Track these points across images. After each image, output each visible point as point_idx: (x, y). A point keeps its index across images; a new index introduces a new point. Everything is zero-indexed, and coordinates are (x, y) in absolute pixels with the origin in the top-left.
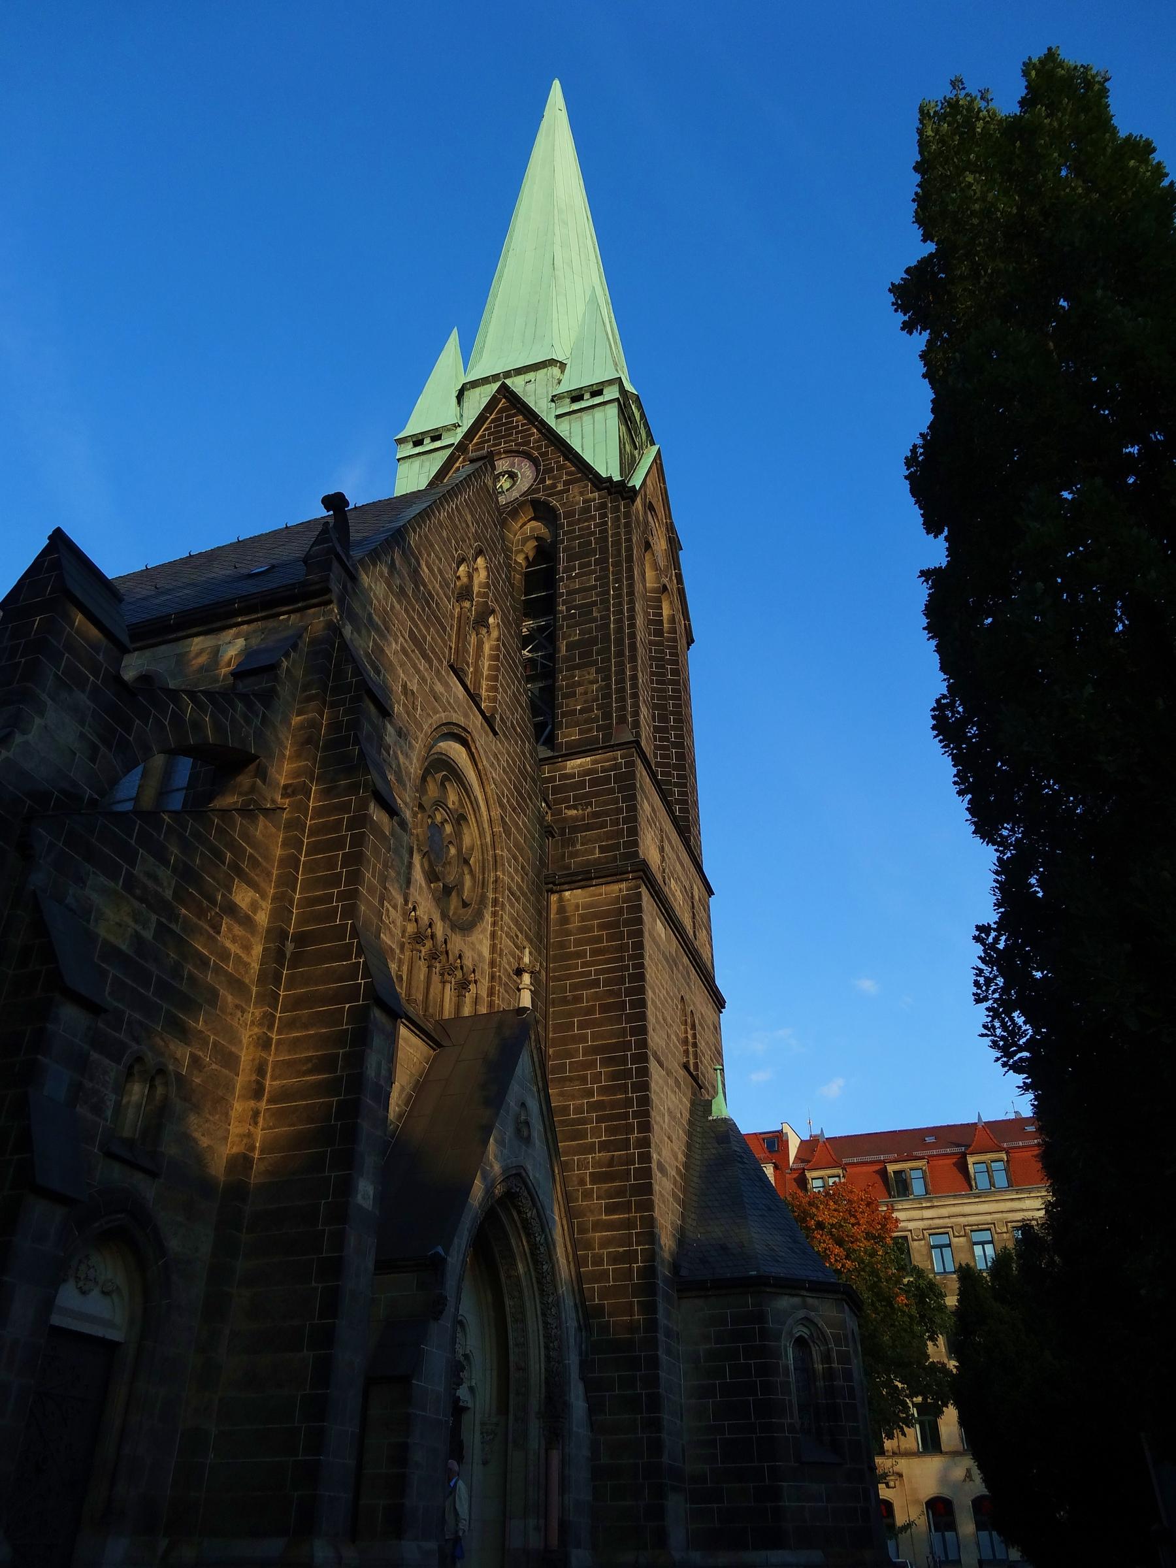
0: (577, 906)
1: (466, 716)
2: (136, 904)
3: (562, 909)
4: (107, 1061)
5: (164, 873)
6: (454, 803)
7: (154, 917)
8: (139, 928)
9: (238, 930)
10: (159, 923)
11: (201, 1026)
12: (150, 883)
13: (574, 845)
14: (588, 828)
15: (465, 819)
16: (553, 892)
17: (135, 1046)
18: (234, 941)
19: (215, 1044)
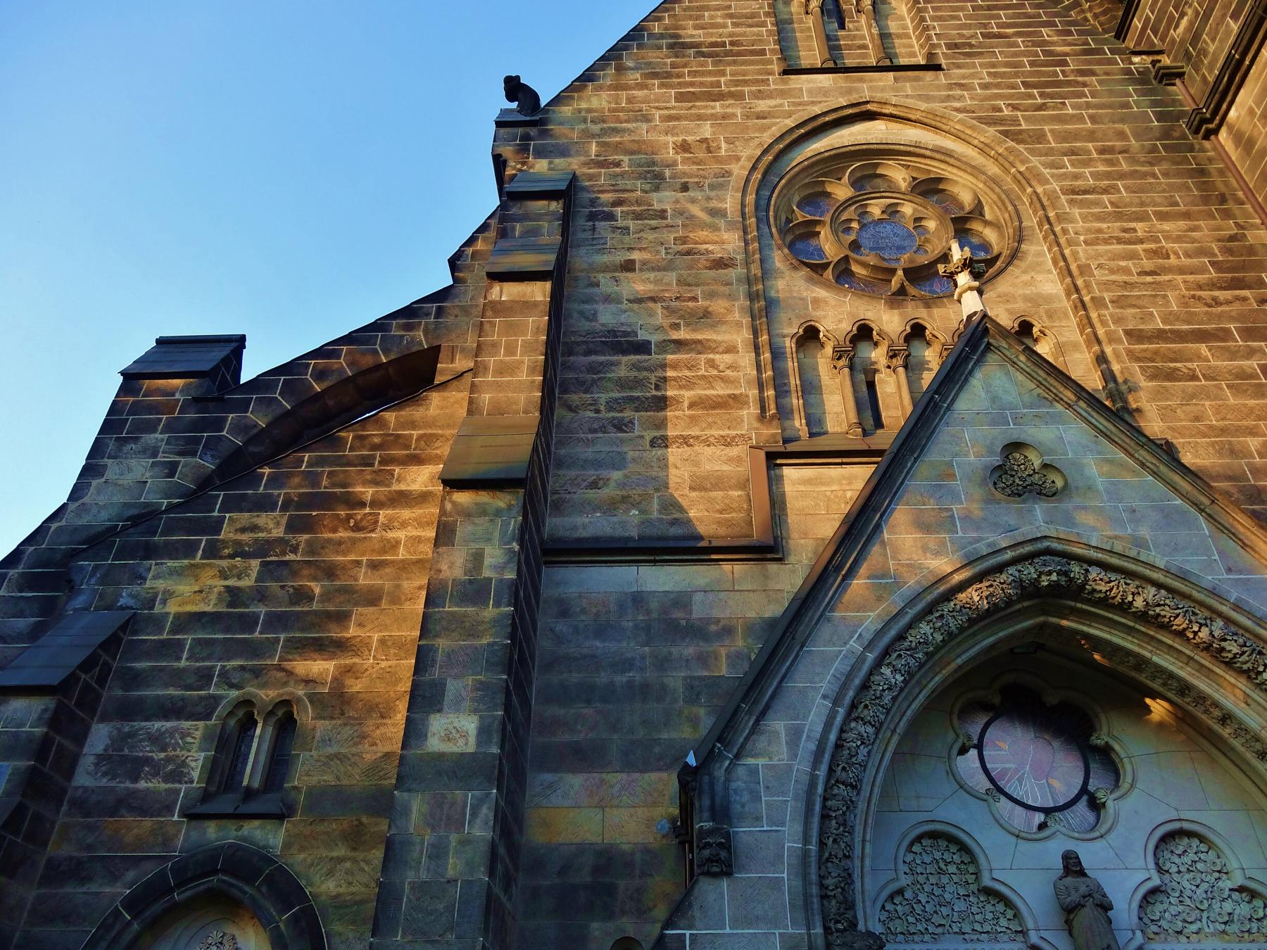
0: (1251, 112)
1: (849, 91)
2: (224, 563)
3: (1238, 137)
4: (186, 724)
5: (264, 519)
6: (904, 179)
7: (255, 564)
8: (230, 582)
9: (406, 514)
10: (264, 565)
11: (352, 631)
12: (245, 537)
13: (1203, 52)
14: (1207, 16)
15: (940, 180)
16: (1216, 131)
17: (234, 693)
18: (404, 525)
19: (382, 641)
